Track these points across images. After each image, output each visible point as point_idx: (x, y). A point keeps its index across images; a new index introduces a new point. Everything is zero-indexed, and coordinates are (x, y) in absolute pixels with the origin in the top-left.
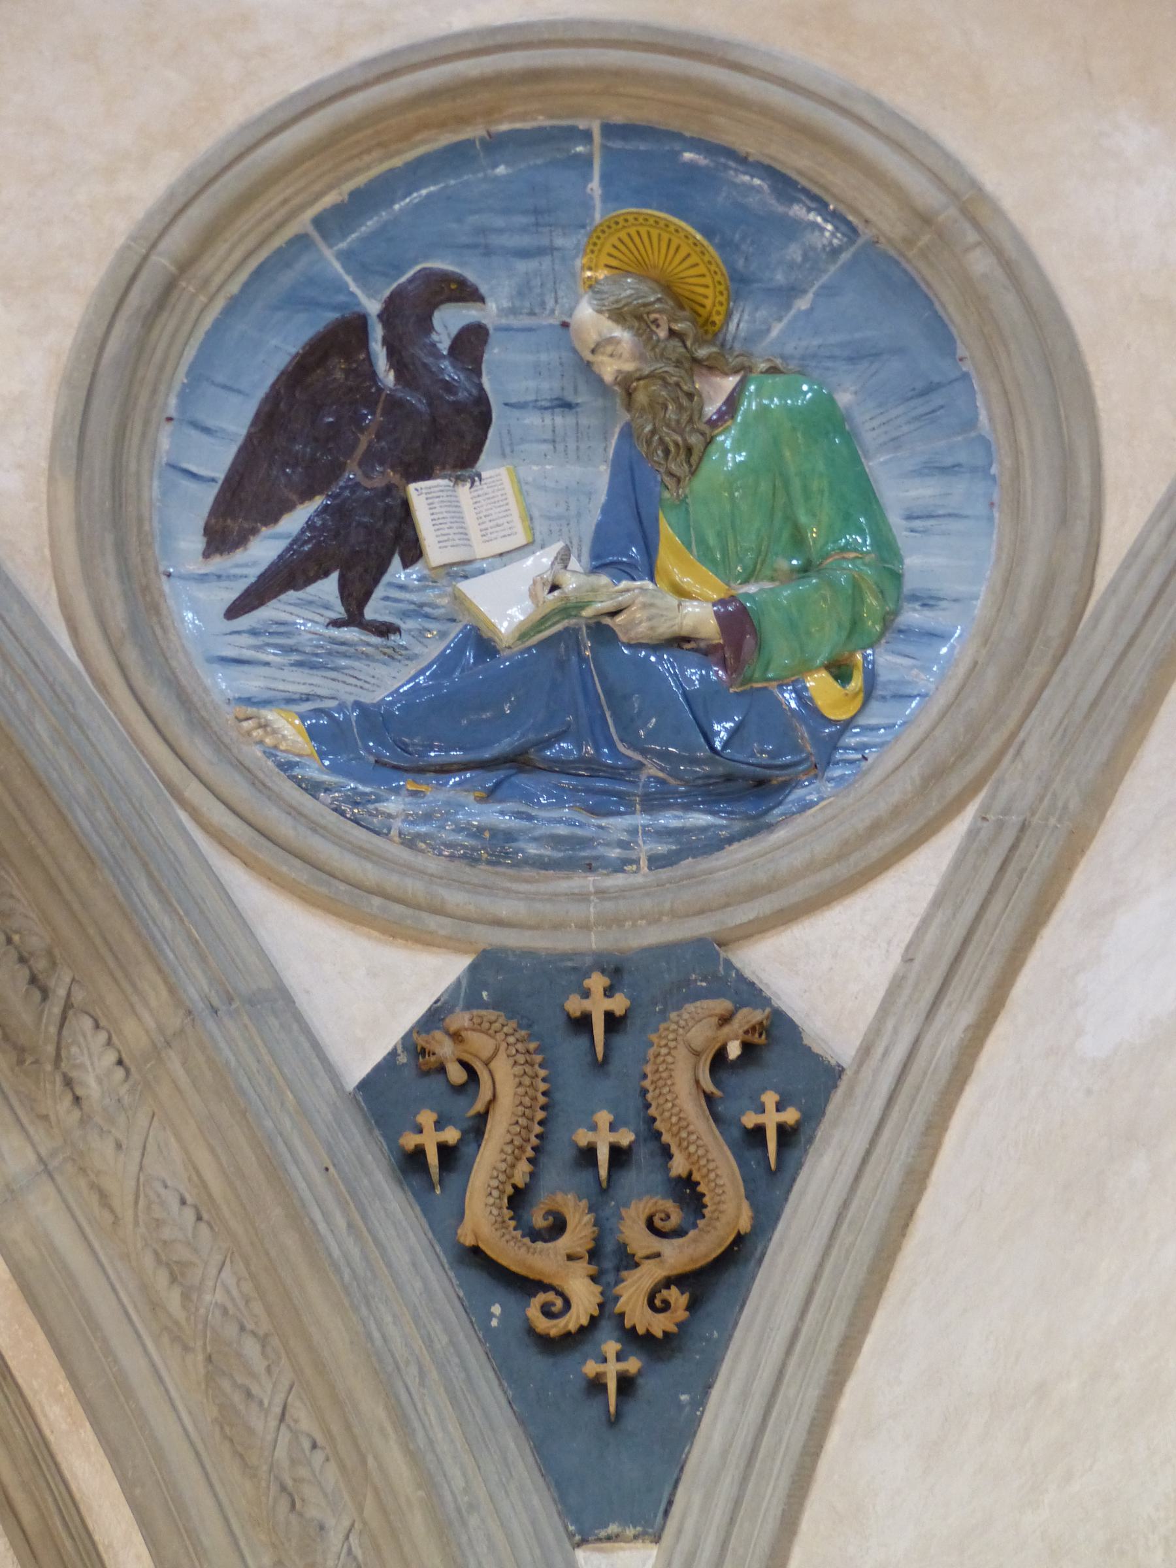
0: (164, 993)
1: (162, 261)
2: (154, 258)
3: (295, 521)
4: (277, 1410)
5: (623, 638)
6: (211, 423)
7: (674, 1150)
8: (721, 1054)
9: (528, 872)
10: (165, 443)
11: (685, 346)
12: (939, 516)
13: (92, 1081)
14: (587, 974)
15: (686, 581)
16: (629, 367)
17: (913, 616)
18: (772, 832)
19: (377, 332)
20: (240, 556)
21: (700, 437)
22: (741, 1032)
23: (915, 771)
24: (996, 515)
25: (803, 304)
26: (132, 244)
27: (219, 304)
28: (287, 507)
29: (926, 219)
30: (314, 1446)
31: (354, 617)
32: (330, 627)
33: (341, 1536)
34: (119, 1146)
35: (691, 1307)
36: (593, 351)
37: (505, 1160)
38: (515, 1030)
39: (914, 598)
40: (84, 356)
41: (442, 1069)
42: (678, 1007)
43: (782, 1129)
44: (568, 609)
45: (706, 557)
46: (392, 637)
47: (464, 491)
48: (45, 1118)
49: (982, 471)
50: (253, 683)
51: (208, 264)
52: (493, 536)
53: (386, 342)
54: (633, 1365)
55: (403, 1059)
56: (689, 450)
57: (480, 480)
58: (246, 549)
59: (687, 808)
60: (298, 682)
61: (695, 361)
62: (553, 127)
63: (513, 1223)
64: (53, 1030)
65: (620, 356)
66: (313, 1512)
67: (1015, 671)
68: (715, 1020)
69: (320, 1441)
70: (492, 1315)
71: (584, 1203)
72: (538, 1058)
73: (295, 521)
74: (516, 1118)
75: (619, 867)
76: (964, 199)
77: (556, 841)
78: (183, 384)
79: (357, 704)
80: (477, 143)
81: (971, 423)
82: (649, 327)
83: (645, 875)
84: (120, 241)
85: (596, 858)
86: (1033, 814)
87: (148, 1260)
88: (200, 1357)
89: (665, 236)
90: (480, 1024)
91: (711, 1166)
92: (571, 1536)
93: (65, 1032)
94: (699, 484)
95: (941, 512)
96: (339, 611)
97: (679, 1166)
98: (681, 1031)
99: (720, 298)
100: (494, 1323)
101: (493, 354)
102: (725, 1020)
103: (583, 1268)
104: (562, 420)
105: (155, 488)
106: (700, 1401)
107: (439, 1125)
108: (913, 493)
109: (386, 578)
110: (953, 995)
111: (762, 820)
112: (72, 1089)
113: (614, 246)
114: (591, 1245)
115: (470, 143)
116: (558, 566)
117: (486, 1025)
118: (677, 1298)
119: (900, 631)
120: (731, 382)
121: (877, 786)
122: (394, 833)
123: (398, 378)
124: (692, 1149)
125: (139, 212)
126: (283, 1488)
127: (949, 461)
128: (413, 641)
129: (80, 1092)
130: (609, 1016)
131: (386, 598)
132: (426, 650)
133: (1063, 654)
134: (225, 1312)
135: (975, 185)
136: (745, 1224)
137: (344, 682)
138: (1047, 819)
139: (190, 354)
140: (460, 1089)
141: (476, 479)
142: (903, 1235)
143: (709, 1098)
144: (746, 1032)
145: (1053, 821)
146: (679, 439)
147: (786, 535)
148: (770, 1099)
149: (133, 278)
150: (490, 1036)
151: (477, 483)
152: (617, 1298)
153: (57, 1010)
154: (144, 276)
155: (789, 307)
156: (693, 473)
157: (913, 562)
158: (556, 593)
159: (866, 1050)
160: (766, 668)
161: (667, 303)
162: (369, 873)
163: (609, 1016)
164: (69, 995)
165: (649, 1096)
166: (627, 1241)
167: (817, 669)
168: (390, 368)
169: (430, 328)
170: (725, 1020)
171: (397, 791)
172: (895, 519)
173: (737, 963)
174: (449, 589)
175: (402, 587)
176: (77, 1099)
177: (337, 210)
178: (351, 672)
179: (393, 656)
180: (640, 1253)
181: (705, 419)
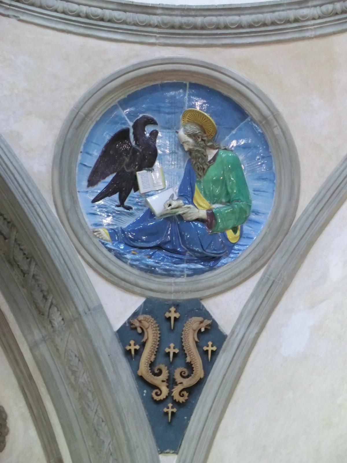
0: (74, 309)
1: (82, 114)
2: (80, 113)
3: (109, 179)
4: (95, 411)
5: (185, 219)
6: (91, 152)
7: (188, 355)
8: (200, 330)
9: (158, 276)
10: (80, 157)
11: (205, 143)
12: (261, 191)
13: (56, 324)
14: (170, 307)
15: (201, 204)
16: (191, 147)
17: (253, 217)
18: (216, 270)
19: (132, 131)
20: (96, 187)
21: (207, 166)
22: (205, 325)
23: (250, 260)
24: (275, 193)
25: (234, 132)
26: (75, 109)
27: (94, 123)
28: (108, 175)
29: (265, 118)
30: (103, 421)
32: (116, 207)
33: (108, 444)
34: (62, 339)
35: (188, 396)
36: (183, 143)
37: (149, 355)
38: (153, 321)
39: (253, 212)
40: (62, 138)
41: (135, 328)
42: (191, 317)
43: (212, 351)
45: (205, 196)
46: (130, 210)
47: (149, 173)
48: (45, 327)
49: (272, 181)
51: (93, 114)
52: (156, 185)
53: (134, 133)
54: (175, 410)
55: (127, 325)
56: (204, 169)
57: (154, 171)
58: (97, 185)
59: (196, 263)
61: (207, 146)
62: (177, 82)
63: (150, 371)
64: (48, 309)
65: (189, 145)
66: (101, 437)
67: (275, 237)
68: (199, 322)
69: (104, 420)
70: (144, 393)
71: (166, 367)
72: (158, 328)
73: (109, 179)
74: (153, 345)
75: (179, 277)
76: (274, 114)
77: (166, 270)
78: (85, 143)
79: (121, 228)
80: (159, 85)
82: (196, 138)
83: (185, 279)
84: (72, 107)
85: (174, 274)
86: (276, 279)
87: (67, 368)
88: (78, 393)
89: (202, 116)
90: (145, 319)
91: (196, 361)
92: (158, 451)
93: (51, 311)
94: (205, 178)
95: (261, 190)
96: (118, 203)
97: (188, 360)
98: (191, 325)
99: (214, 131)
100: (144, 395)
102: (201, 322)
103: (165, 384)
106: (189, 419)
107: (135, 345)
108: (255, 184)
109: (130, 195)
110: (253, 324)
111: (214, 267)
112: (52, 324)
113: (190, 115)
114: (167, 378)
115: (157, 85)
116: (171, 200)
117: (147, 320)
118: (186, 394)
119: (250, 220)
120: (215, 152)
121: (241, 261)
122: (128, 263)
123: (136, 143)
124: (192, 356)
125: (77, 100)
126: (95, 430)
127: (265, 177)
128: (135, 212)
129: (54, 325)
130: (175, 318)
131: (130, 200)
132: (138, 214)
133: (287, 234)
134: (84, 385)
135: (277, 111)
136: (202, 376)
137: (119, 221)
138: (279, 281)
139: (87, 135)
140: (140, 334)
141: (153, 170)
142: (237, 383)
143: (196, 342)
144: (206, 326)
145: (280, 282)
146: (201, 166)
147: (225, 193)
148: (210, 343)
149: (75, 117)
150: (147, 322)
151: (153, 172)
152: (172, 392)
153: (49, 305)
154: (77, 117)
155: (230, 132)
156: (204, 174)
157: (254, 202)
158: (170, 207)
159: (233, 332)
160: (217, 229)
161: (201, 133)
163: (175, 318)
164: (52, 301)
165: (183, 340)
166: (175, 375)
167: (230, 229)
168: (134, 140)
169: (144, 131)
170: (201, 322)
171: (129, 253)
172: (251, 191)
173: (205, 306)
174: (145, 199)
175: (133, 197)
176: (52, 327)
178: (120, 219)
179: (131, 214)
180: (178, 382)
181: (208, 161)
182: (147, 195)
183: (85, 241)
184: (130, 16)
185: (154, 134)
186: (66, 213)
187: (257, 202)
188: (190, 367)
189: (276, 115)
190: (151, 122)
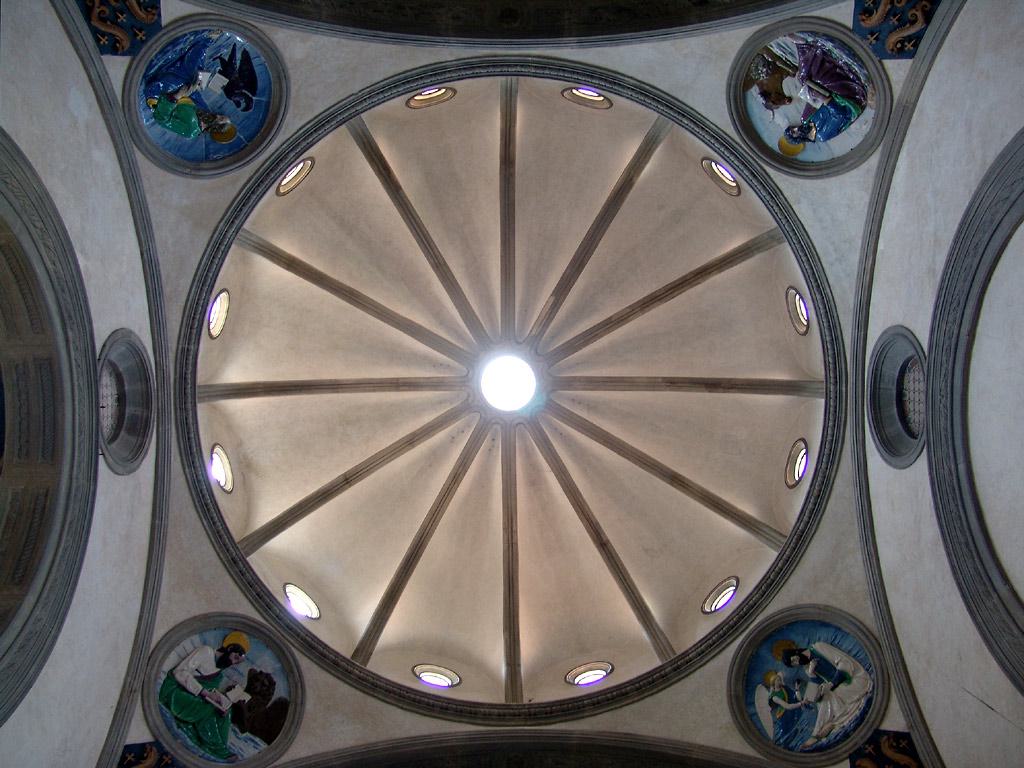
1: (284, 81)
10: (263, 58)
29: (199, 170)
31: (220, 57)
35: (87, 5)
44: (194, 83)
50: (223, 38)
60: (219, 43)
75: (156, 55)
81: (170, 149)
101: (234, 106)
104: (219, 105)
105: (259, 52)
162: (187, 27)
170: (123, 48)
177: (269, 106)
179: (211, 57)
182: (212, 76)
183: (223, 24)
184: (304, 144)
185: (238, 104)
186: (246, 28)
187: (158, 128)
188: (103, 20)
189: (196, 177)
190: (244, 110)
